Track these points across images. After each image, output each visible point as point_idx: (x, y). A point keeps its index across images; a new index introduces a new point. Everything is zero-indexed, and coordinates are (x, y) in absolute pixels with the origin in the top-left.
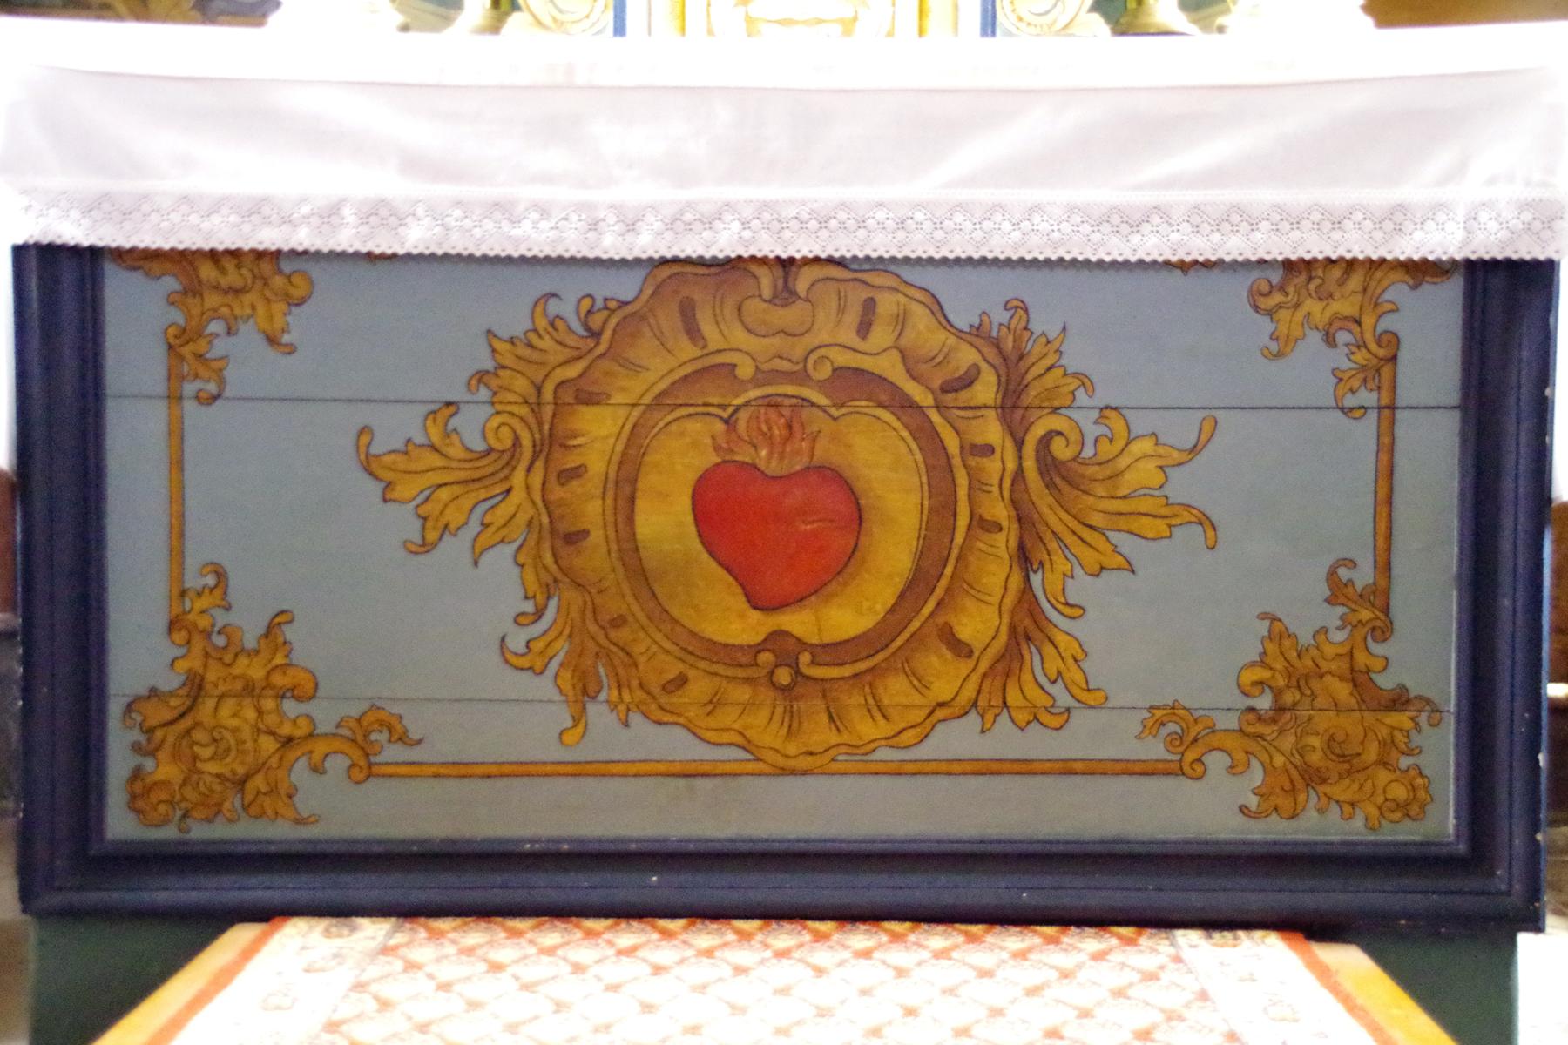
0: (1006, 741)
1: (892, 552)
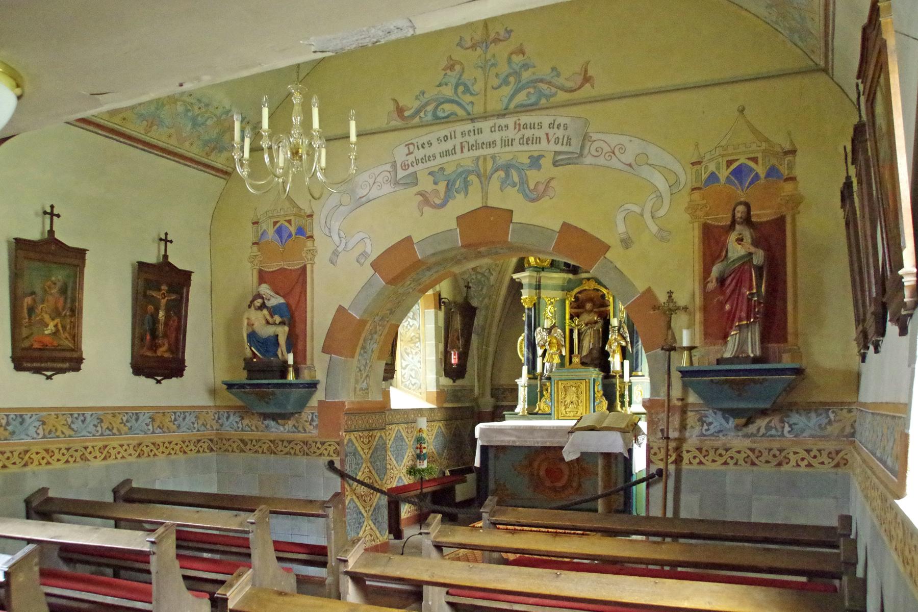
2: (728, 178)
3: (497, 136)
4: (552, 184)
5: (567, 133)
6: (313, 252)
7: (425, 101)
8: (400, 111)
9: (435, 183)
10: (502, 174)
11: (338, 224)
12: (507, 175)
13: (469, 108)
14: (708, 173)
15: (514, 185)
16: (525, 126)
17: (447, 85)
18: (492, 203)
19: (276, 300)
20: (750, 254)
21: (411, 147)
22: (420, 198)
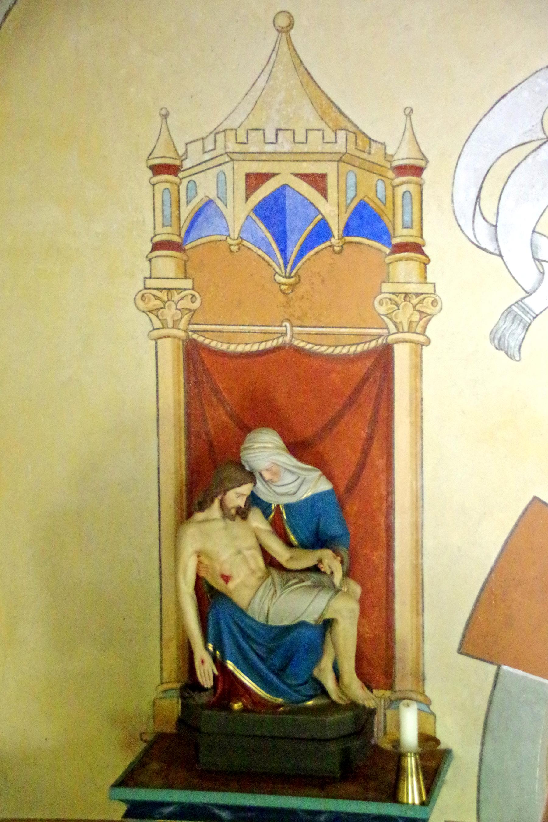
6: (423, 304)
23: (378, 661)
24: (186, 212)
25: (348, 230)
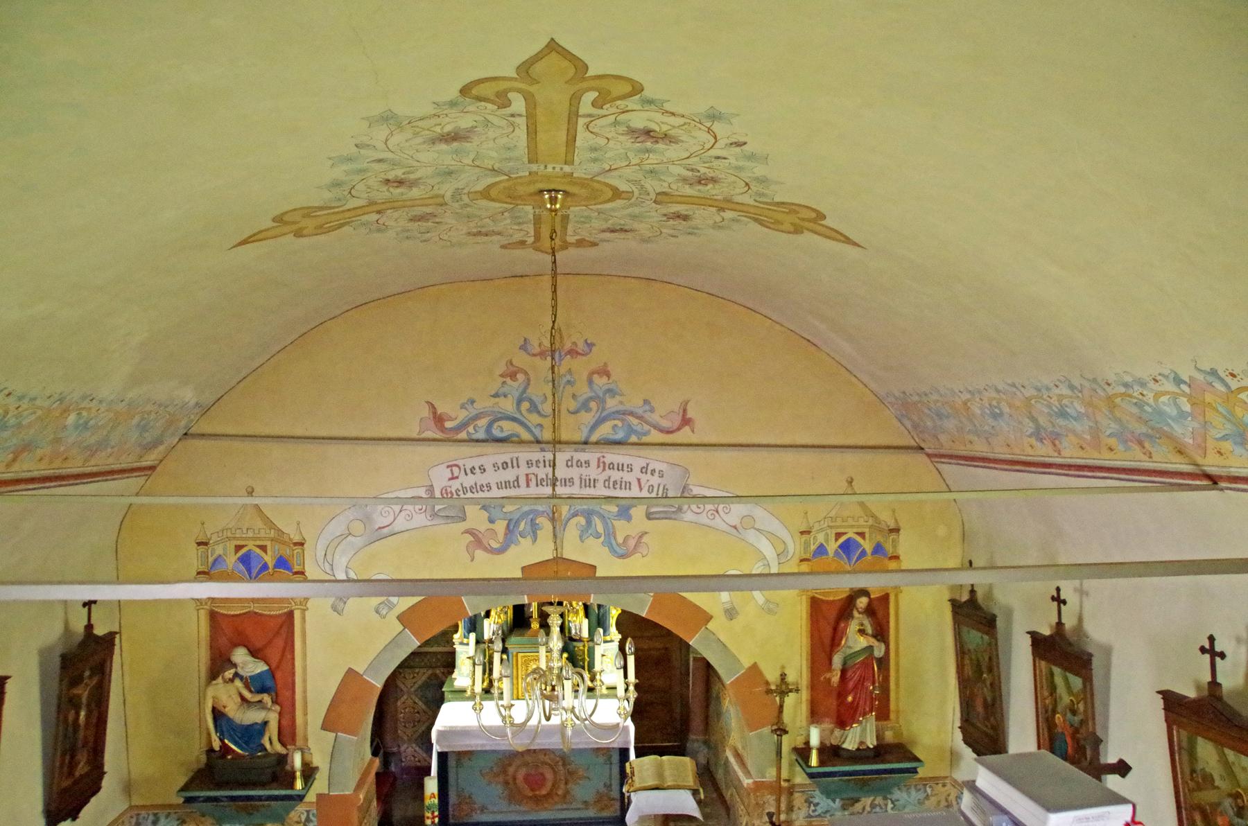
0: (565, 806)
1: (549, 784)
2: (836, 552)
3: (574, 473)
4: (645, 539)
5: (663, 481)
7: (474, 412)
8: (439, 420)
9: (492, 521)
10: (581, 520)
11: (344, 560)
12: (589, 522)
13: (537, 431)
14: (817, 544)
15: (598, 536)
16: (611, 466)
17: (505, 396)
18: (570, 553)
19: (255, 668)
20: (870, 648)
21: (456, 470)
22: (470, 538)
23: (288, 734)
24: (211, 560)
25: (275, 566)
